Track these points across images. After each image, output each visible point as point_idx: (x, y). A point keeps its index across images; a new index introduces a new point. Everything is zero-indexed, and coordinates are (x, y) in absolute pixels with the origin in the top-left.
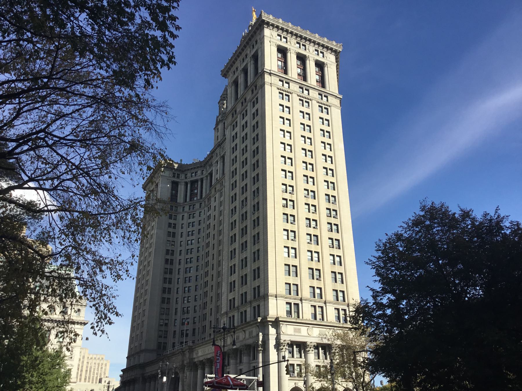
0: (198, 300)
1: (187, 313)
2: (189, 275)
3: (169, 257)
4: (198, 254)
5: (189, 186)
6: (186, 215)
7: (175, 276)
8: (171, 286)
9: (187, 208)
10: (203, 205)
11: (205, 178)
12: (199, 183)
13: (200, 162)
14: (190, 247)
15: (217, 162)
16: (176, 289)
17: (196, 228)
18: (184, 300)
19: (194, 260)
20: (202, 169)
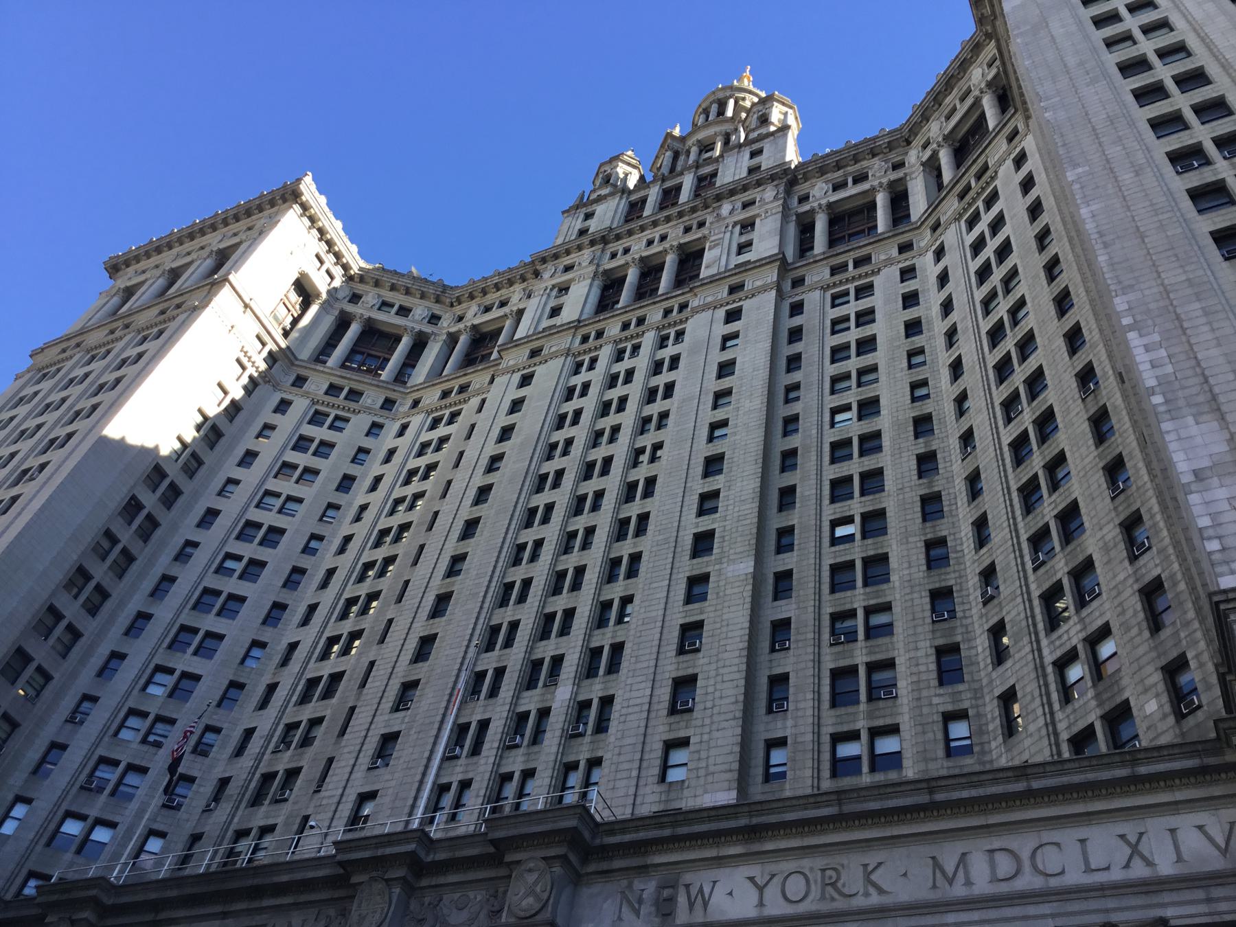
0: (222, 748)
1: (113, 794)
2: (209, 622)
3: (150, 500)
4: (305, 562)
5: (354, 330)
6: (300, 406)
7: (131, 596)
8: (88, 626)
9: (317, 384)
10: (404, 406)
11: (444, 337)
13: (445, 288)
14: (269, 518)
16: (103, 651)
17: (331, 468)
18: (122, 726)
19: (272, 578)
20: (437, 309)
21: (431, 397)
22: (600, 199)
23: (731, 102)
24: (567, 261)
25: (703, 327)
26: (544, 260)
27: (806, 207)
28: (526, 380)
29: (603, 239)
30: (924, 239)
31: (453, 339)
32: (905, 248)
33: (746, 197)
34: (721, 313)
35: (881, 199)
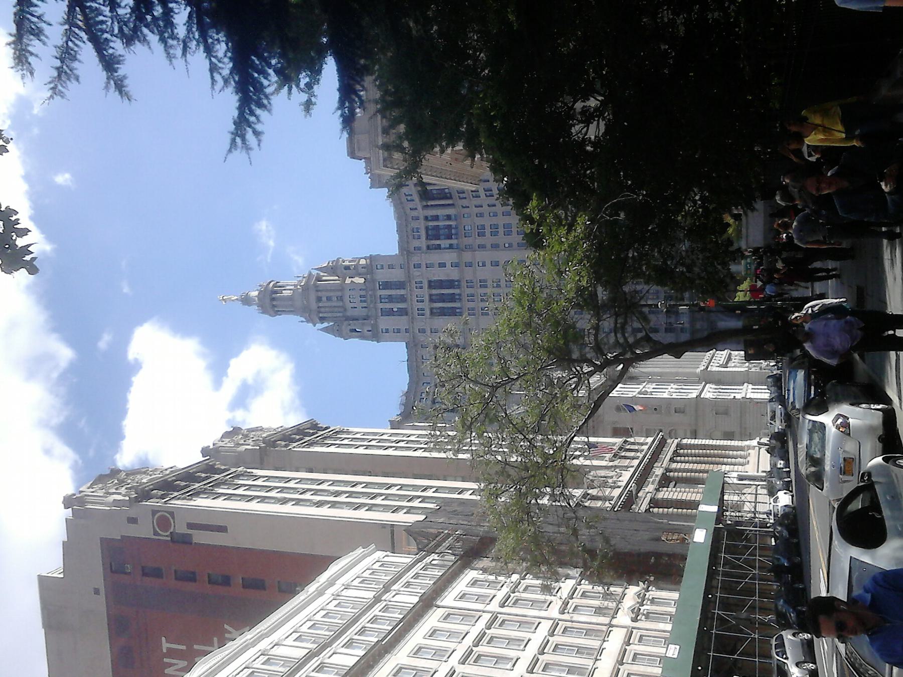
25: (486, 273)
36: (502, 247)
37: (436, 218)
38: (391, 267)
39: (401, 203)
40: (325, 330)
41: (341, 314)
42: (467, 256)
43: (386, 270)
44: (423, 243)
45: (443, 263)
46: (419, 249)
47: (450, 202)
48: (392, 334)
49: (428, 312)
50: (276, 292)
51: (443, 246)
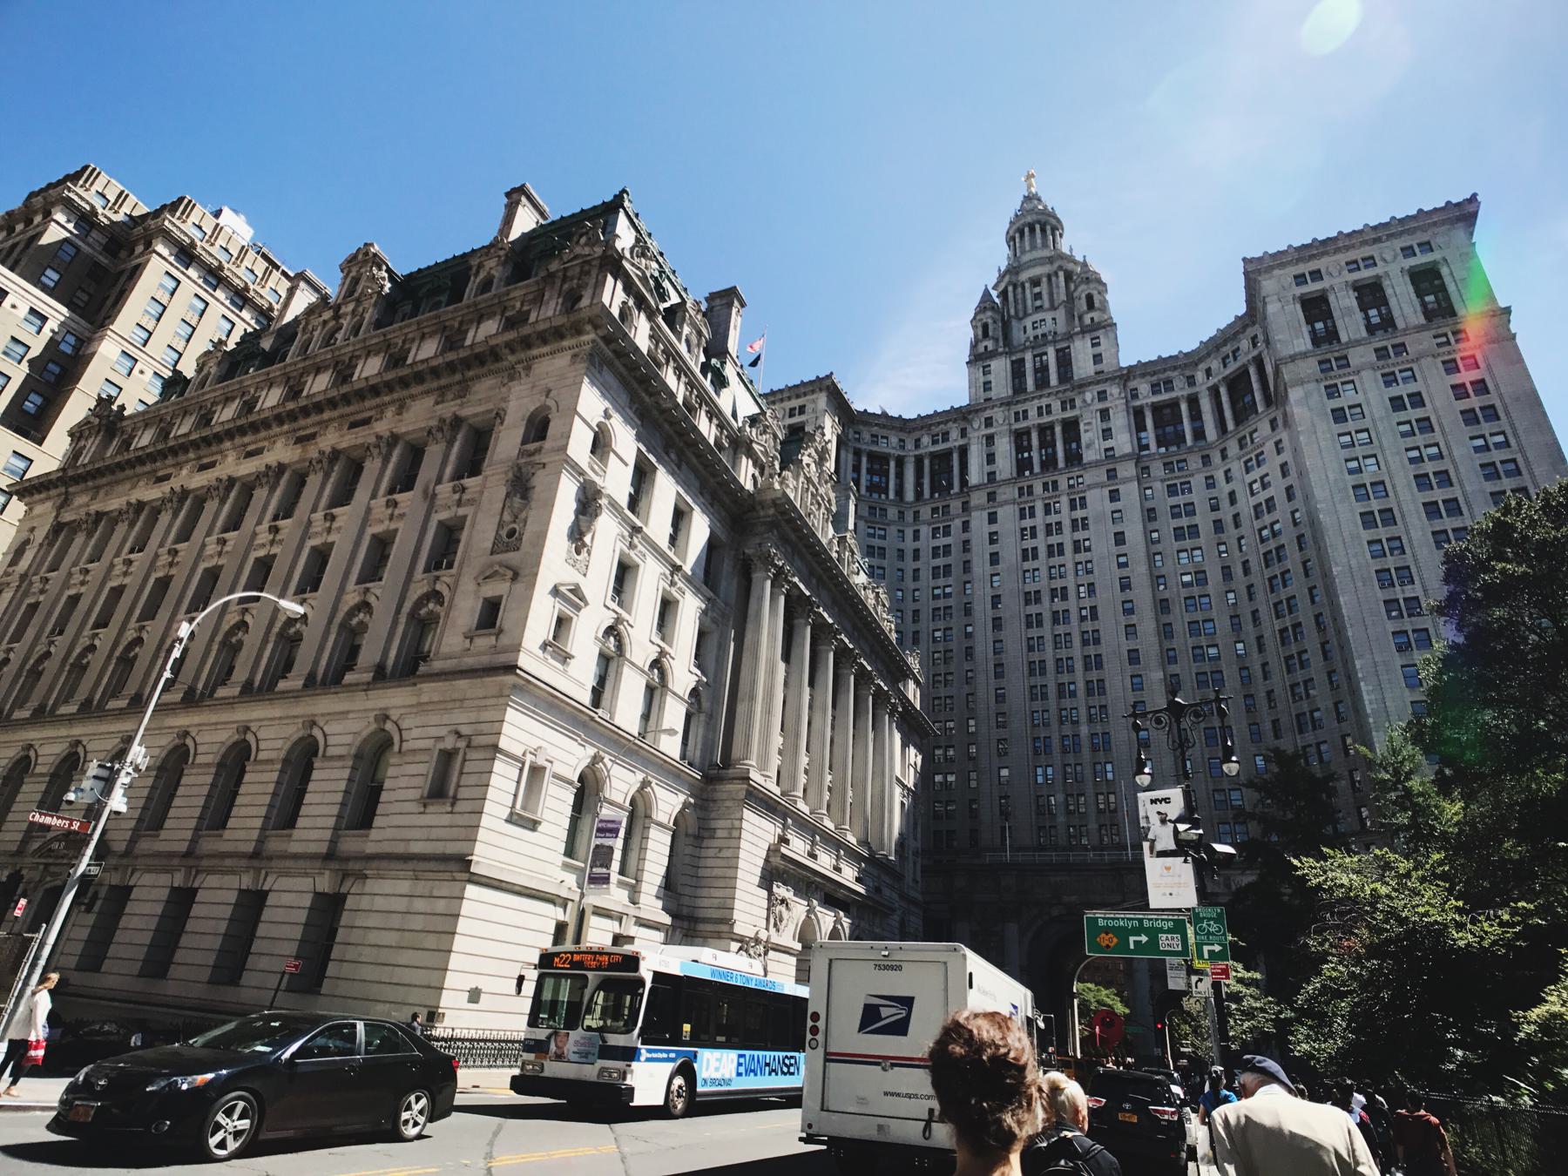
5: (864, 460)
12: (892, 464)
15: (990, 439)
21: (925, 512)
22: (993, 355)
23: (1038, 227)
24: (988, 414)
25: (1097, 501)
26: (970, 412)
27: (1138, 403)
28: (992, 518)
29: (1006, 403)
30: (1216, 457)
31: (919, 461)
32: (1206, 460)
33: (1100, 388)
34: (1106, 492)
35: (1184, 407)
36: (1151, 526)
37: (1196, 415)
38: (1097, 358)
39: (1218, 348)
40: (986, 293)
41: (1012, 312)
42: (1127, 470)
43: (1090, 351)
44: (1146, 397)
45: (1110, 433)
46: (1135, 396)
47: (1230, 426)
48: (982, 379)
49: (1022, 424)
50: (1043, 231)
51: (1143, 435)
